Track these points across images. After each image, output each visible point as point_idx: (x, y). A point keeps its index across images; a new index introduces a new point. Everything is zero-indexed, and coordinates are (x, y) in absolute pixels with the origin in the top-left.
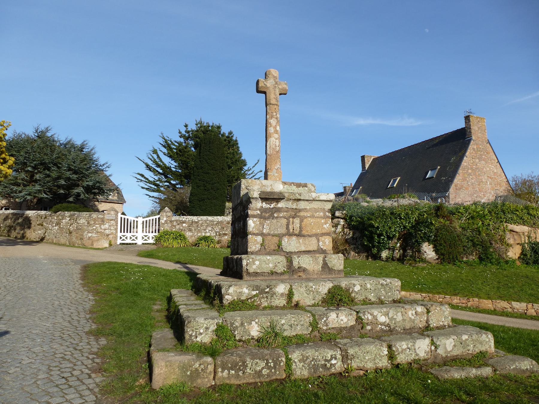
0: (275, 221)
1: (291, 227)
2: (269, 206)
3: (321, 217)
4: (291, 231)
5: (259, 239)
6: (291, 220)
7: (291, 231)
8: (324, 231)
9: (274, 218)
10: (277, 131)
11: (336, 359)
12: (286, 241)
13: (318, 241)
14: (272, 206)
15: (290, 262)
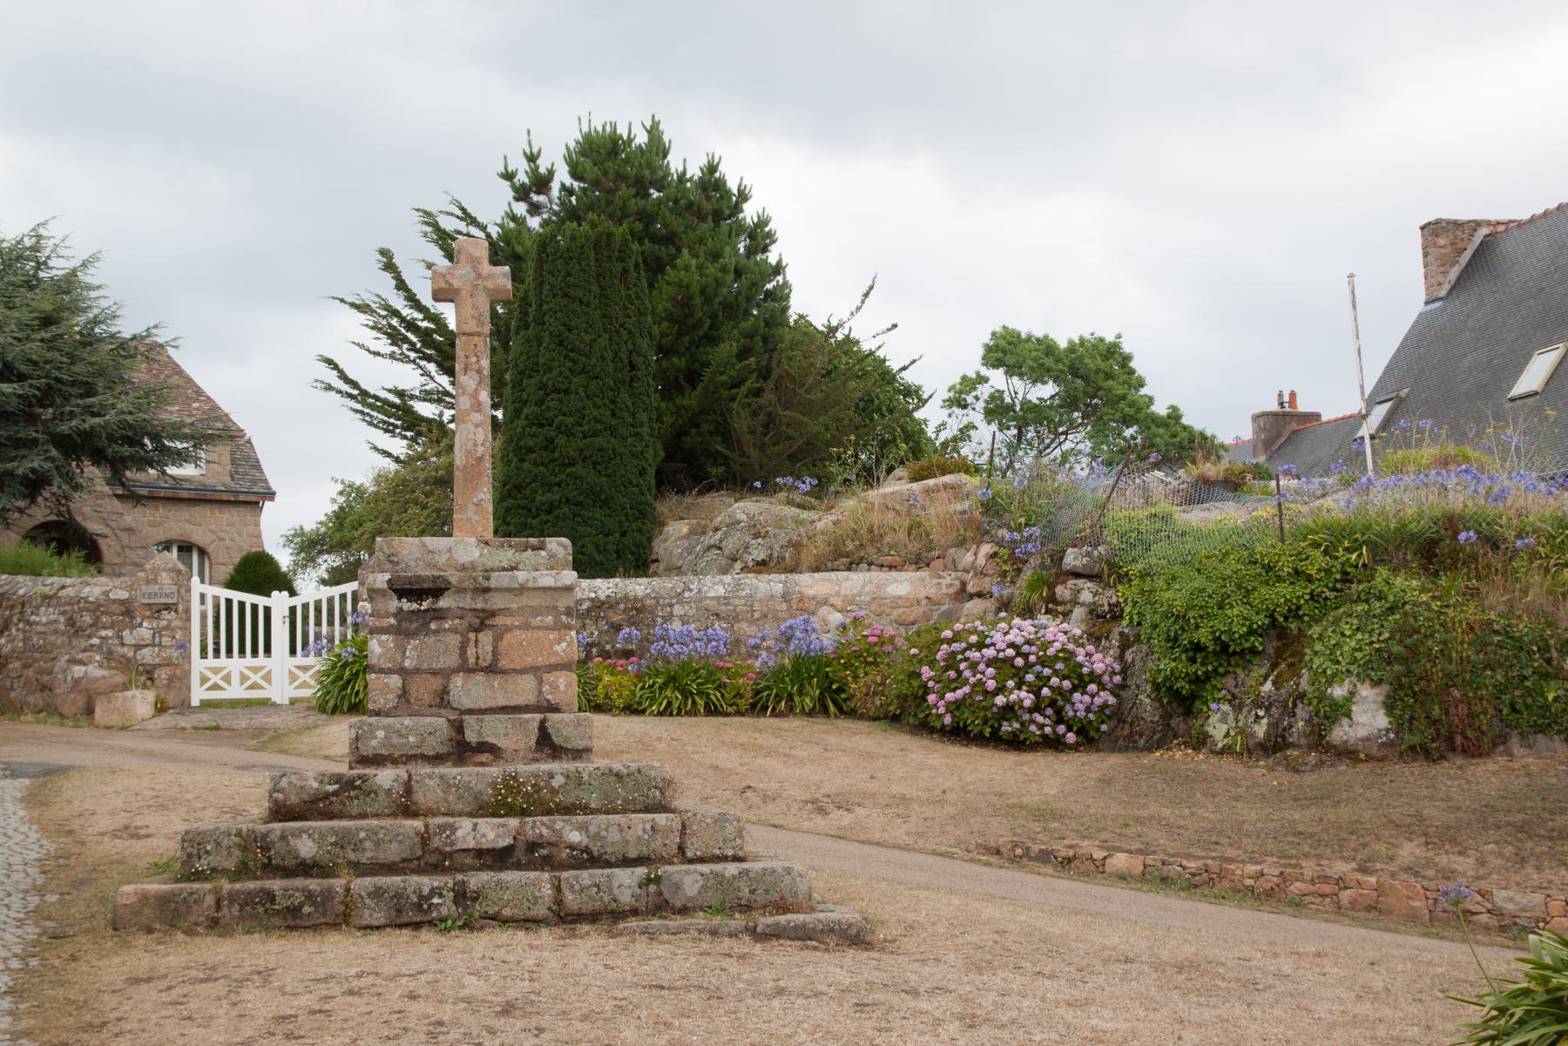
0: (431, 640)
1: (471, 651)
2: (415, 606)
3: (547, 628)
4: (472, 661)
5: (395, 681)
6: (472, 635)
7: (472, 661)
8: (553, 660)
9: (428, 632)
10: (479, 404)
11: (441, 895)
12: (460, 683)
13: (541, 682)
14: (425, 605)
15: (458, 727)
